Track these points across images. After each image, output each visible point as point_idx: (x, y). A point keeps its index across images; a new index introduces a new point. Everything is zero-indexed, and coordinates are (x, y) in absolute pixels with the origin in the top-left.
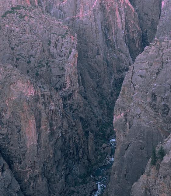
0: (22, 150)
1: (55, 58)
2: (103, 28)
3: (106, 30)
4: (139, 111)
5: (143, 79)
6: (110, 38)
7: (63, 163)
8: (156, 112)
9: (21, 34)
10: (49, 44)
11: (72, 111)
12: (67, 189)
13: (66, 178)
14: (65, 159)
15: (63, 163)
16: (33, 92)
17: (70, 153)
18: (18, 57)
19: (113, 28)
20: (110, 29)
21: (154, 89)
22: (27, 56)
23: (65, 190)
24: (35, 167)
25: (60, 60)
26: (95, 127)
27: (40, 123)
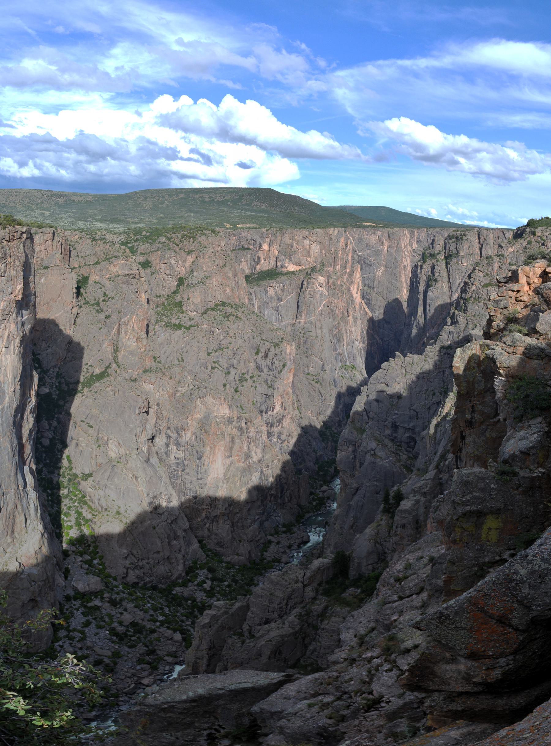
0: (200, 482)
1: (263, 371)
2: (331, 338)
3: (335, 339)
4: (373, 445)
5: (380, 404)
6: (340, 351)
7: (259, 506)
8: (398, 446)
9: (222, 337)
10: (257, 353)
11: (280, 442)
12: (261, 538)
13: (261, 524)
14: (262, 501)
15: (259, 506)
16: (227, 411)
17: (272, 495)
18: (214, 365)
19: (345, 338)
20: (341, 340)
21: (394, 417)
22: (226, 365)
23: (259, 538)
24: (215, 506)
25: (269, 375)
26: (312, 464)
27: (231, 453)
